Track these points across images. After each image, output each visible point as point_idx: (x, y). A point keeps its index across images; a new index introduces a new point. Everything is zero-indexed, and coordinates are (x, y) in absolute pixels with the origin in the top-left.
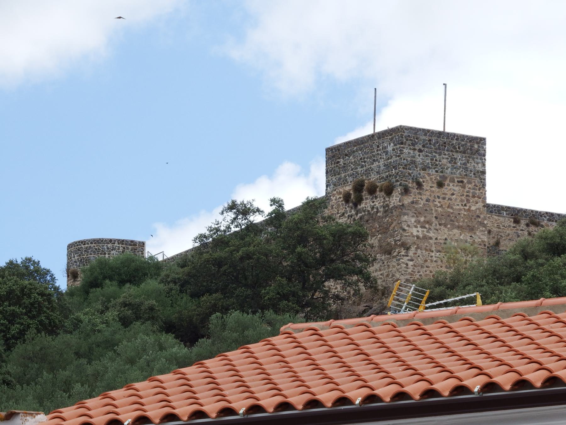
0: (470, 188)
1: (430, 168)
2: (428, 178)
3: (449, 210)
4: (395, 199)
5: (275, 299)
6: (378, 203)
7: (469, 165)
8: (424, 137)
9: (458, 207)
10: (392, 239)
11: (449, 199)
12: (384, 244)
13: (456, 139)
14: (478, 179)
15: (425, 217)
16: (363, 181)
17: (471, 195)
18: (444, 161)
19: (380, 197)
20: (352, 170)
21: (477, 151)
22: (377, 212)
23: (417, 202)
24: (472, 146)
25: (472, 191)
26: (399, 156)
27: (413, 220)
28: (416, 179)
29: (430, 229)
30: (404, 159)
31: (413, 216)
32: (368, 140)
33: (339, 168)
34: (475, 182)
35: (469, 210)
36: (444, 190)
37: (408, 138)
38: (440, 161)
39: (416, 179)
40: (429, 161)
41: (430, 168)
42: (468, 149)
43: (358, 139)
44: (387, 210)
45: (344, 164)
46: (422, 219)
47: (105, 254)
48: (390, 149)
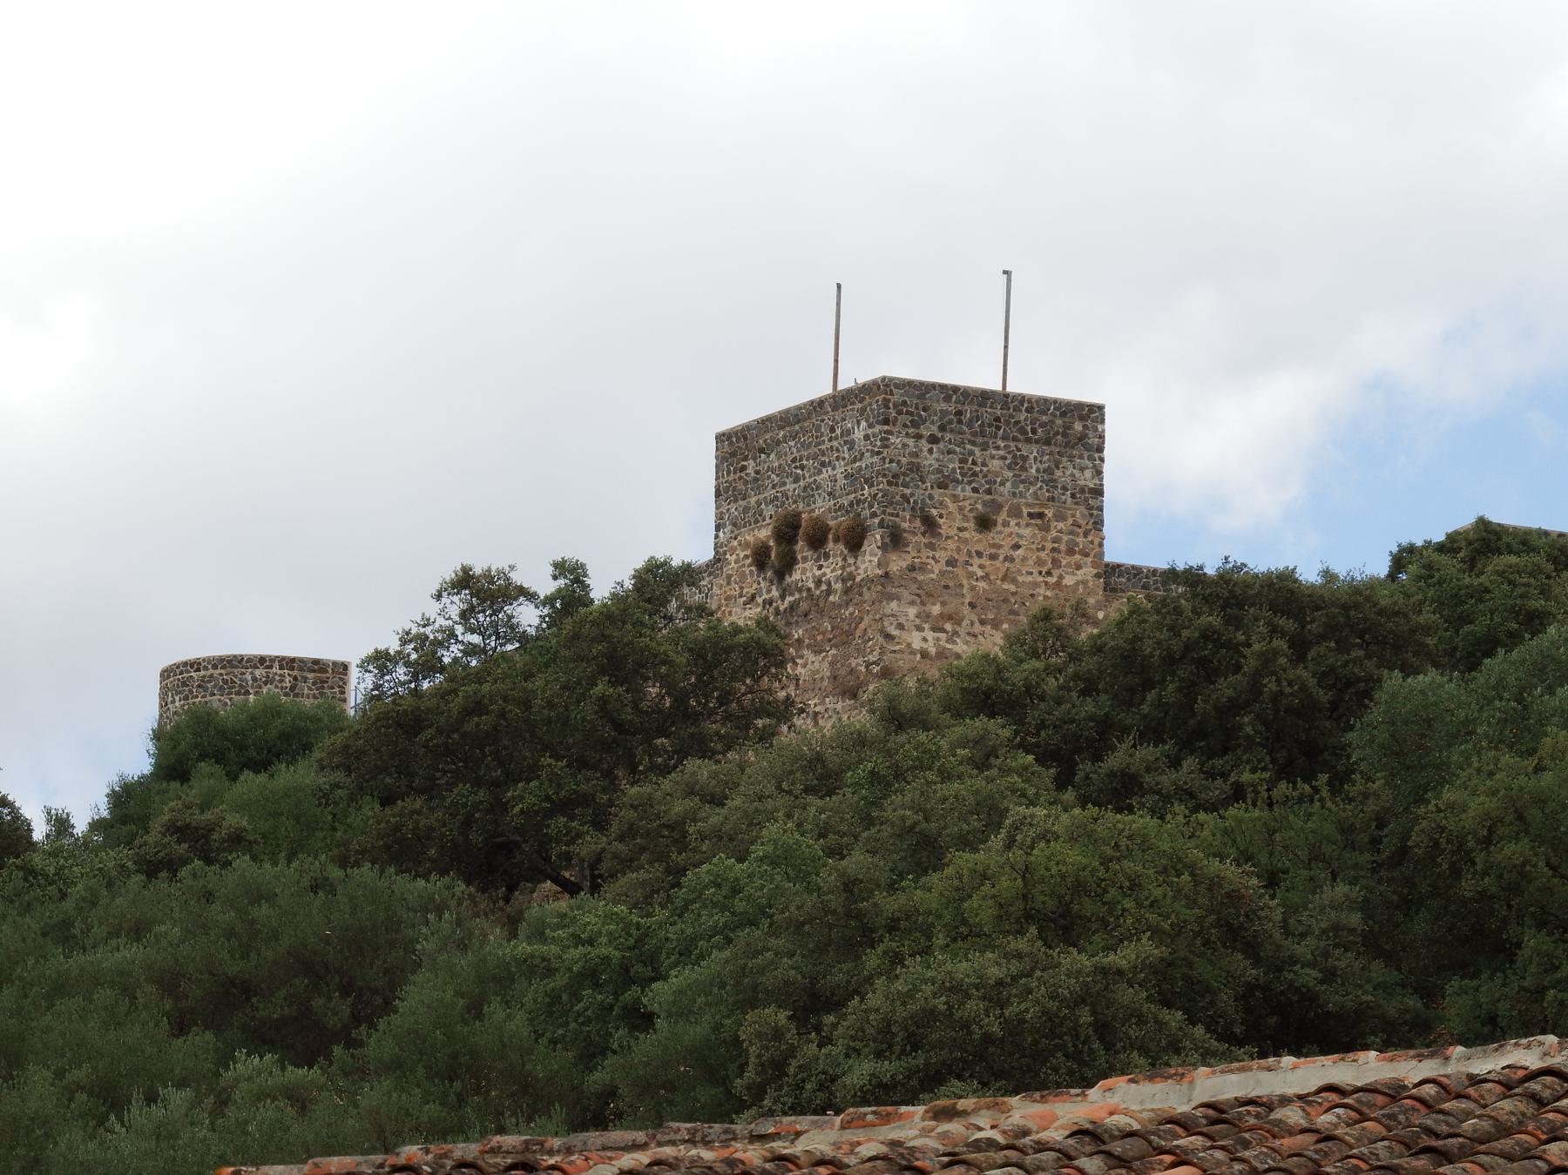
0: (1060, 531)
1: (957, 481)
2: (952, 507)
3: (1006, 586)
4: (869, 562)
5: (537, 813)
6: (831, 571)
7: (1058, 473)
8: (944, 406)
9: (1030, 579)
10: (860, 660)
11: (1006, 558)
12: (842, 672)
13: (1027, 410)
14: (1082, 508)
15: (943, 604)
16: (797, 515)
17: (1063, 547)
18: (995, 464)
19: (835, 556)
20: (774, 487)
21: (1080, 439)
22: (829, 592)
23: (923, 568)
24: (1068, 427)
25: (1066, 538)
26: (878, 453)
27: (912, 612)
28: (922, 509)
29: (955, 633)
30: (891, 461)
31: (912, 603)
32: (810, 413)
33: (746, 482)
34: (1073, 516)
35: (1058, 585)
36: (993, 536)
37: (901, 407)
38: (984, 464)
39: (922, 509)
40: (957, 465)
41: (957, 481)
42: (1057, 433)
43: (787, 411)
44: (852, 588)
45: (757, 472)
46: (936, 609)
47: (248, 693)
48: (858, 435)
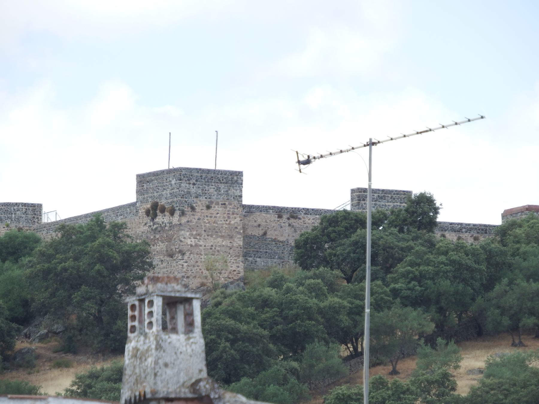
1: (200, 196)
2: (199, 203)
4: (175, 219)
7: (229, 191)
8: (197, 174)
14: (236, 201)
15: (197, 231)
16: (157, 203)
17: (231, 213)
18: (212, 190)
22: (165, 226)
23: (191, 221)
24: (232, 178)
25: (232, 210)
27: (188, 234)
31: (188, 231)
35: (229, 224)
36: (210, 211)
38: (208, 191)
41: (200, 196)
44: (172, 226)
46: (194, 233)
